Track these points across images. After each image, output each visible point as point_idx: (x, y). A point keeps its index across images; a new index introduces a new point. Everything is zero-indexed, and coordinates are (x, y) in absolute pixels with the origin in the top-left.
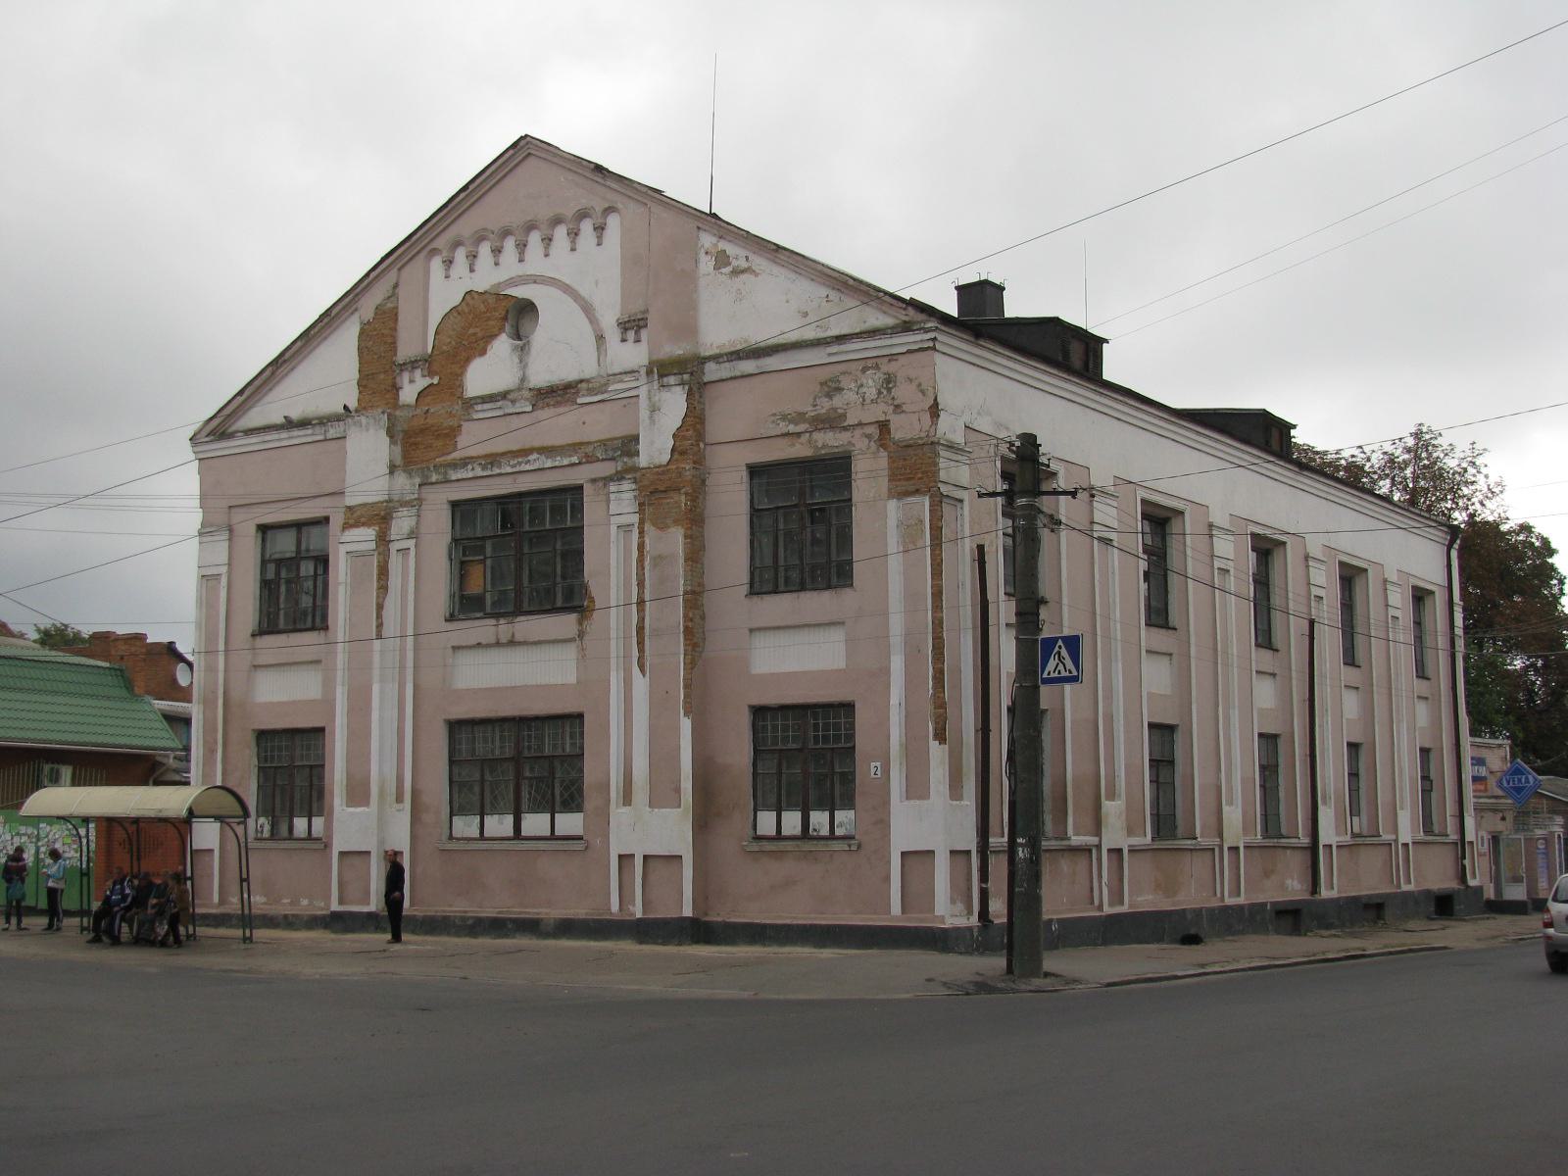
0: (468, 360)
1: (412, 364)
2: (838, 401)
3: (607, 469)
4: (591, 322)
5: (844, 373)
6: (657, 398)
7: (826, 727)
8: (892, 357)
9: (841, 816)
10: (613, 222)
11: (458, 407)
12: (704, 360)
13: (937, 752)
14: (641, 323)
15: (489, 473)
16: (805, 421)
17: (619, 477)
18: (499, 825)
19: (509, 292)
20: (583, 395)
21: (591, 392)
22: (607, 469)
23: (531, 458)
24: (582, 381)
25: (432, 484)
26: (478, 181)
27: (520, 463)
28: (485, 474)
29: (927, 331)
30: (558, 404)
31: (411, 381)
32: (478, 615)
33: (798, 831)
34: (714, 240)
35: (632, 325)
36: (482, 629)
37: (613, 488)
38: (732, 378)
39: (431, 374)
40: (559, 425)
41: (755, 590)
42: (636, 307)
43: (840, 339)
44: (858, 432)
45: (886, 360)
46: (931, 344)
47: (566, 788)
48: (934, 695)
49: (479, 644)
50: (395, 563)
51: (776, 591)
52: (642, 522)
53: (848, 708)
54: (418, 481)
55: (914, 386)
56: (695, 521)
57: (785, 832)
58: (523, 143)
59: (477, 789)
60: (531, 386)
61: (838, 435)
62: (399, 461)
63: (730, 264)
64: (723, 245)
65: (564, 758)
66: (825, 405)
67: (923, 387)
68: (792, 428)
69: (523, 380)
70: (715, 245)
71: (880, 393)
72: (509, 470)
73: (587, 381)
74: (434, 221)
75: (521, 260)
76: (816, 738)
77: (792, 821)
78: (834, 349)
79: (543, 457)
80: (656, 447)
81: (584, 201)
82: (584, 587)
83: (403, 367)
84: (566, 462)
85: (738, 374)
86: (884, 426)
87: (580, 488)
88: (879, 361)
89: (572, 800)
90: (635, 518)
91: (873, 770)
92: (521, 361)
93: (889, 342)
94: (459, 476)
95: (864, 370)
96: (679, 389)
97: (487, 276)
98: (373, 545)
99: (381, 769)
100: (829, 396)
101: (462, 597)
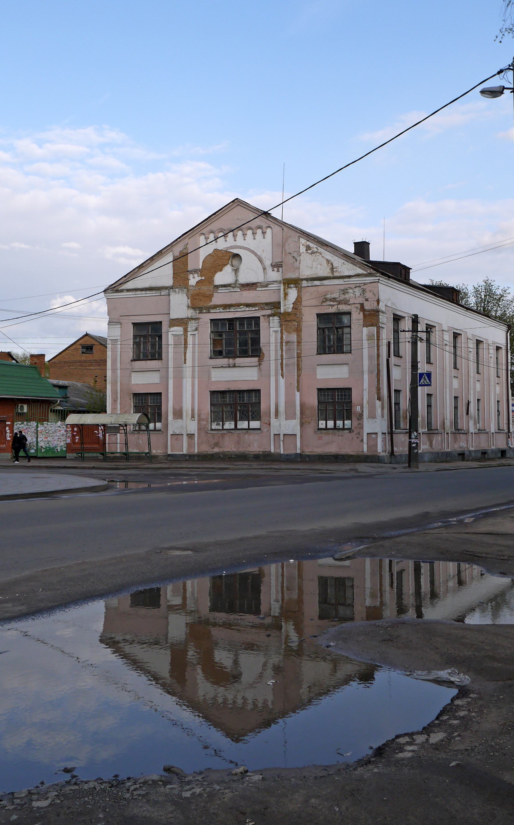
0: (215, 272)
1: (195, 271)
2: (347, 296)
3: (269, 312)
4: (262, 264)
5: (350, 288)
6: (287, 291)
7: (342, 395)
8: (365, 284)
9: (346, 422)
10: (269, 231)
11: (211, 288)
12: (302, 280)
13: (378, 403)
14: (280, 266)
15: (225, 311)
16: (336, 301)
17: (273, 315)
18: (229, 425)
19: (230, 251)
20: (259, 288)
21: (262, 286)
22: (269, 312)
23: (241, 307)
24: (258, 283)
25: (203, 313)
26: (219, 212)
27: (237, 309)
28: (223, 311)
29: (376, 276)
30: (249, 290)
31: (194, 278)
32: (221, 357)
33: (333, 427)
34: (306, 241)
35: (277, 266)
36: (224, 361)
37: (271, 318)
38: (312, 286)
39: (202, 276)
40: (249, 296)
41: (318, 354)
42: (279, 260)
43: (349, 277)
44: (353, 306)
45: (363, 284)
46: (378, 281)
47: (253, 413)
48: (377, 386)
49: (222, 367)
50: (190, 339)
51: (325, 353)
52: (282, 330)
53: (350, 389)
54: (198, 312)
55: (372, 293)
56: (298, 330)
57: (328, 427)
58: (236, 201)
59: (221, 414)
60: (240, 283)
61: (347, 306)
62: (190, 305)
63: (311, 249)
64: (308, 243)
65: (252, 404)
66: (342, 297)
67: (375, 294)
68: (331, 303)
69: (236, 281)
70: (306, 243)
71: (361, 294)
72: (233, 310)
73: (260, 283)
74: (202, 224)
75: (235, 241)
76: (338, 399)
77: (331, 424)
78: (346, 280)
79: (245, 307)
80: (287, 306)
81: (259, 223)
82: (260, 350)
83: (191, 272)
84: (253, 309)
85: (314, 285)
86: (362, 305)
87: (259, 317)
88: (361, 285)
89: (257, 416)
90: (279, 329)
91: (358, 409)
92: (236, 275)
93: (364, 279)
94: (214, 311)
95: (355, 288)
96: (295, 288)
97: (222, 244)
98: (182, 333)
99: (187, 406)
100: (343, 294)
101: (214, 351)
